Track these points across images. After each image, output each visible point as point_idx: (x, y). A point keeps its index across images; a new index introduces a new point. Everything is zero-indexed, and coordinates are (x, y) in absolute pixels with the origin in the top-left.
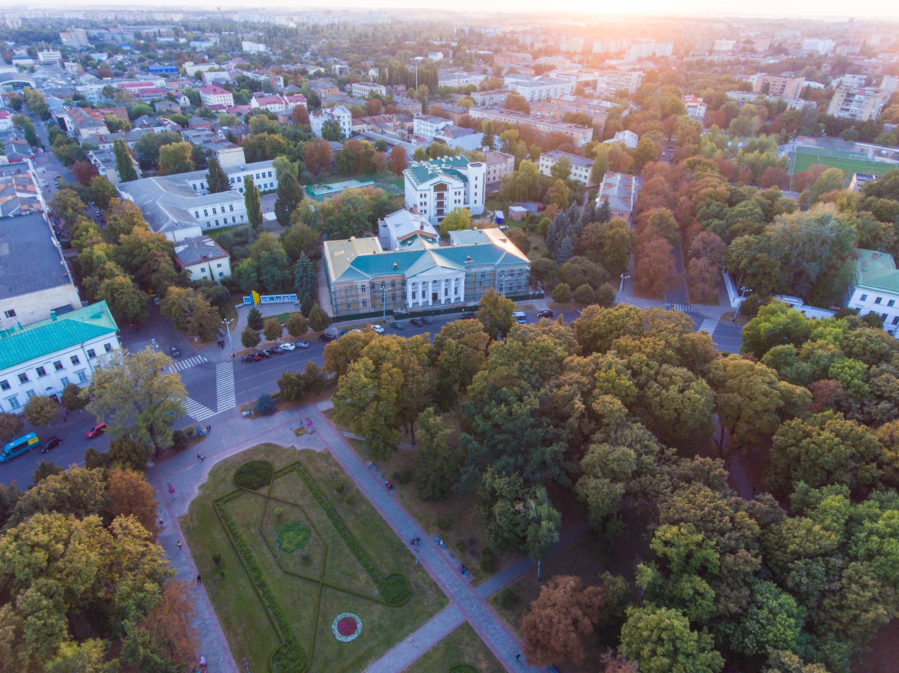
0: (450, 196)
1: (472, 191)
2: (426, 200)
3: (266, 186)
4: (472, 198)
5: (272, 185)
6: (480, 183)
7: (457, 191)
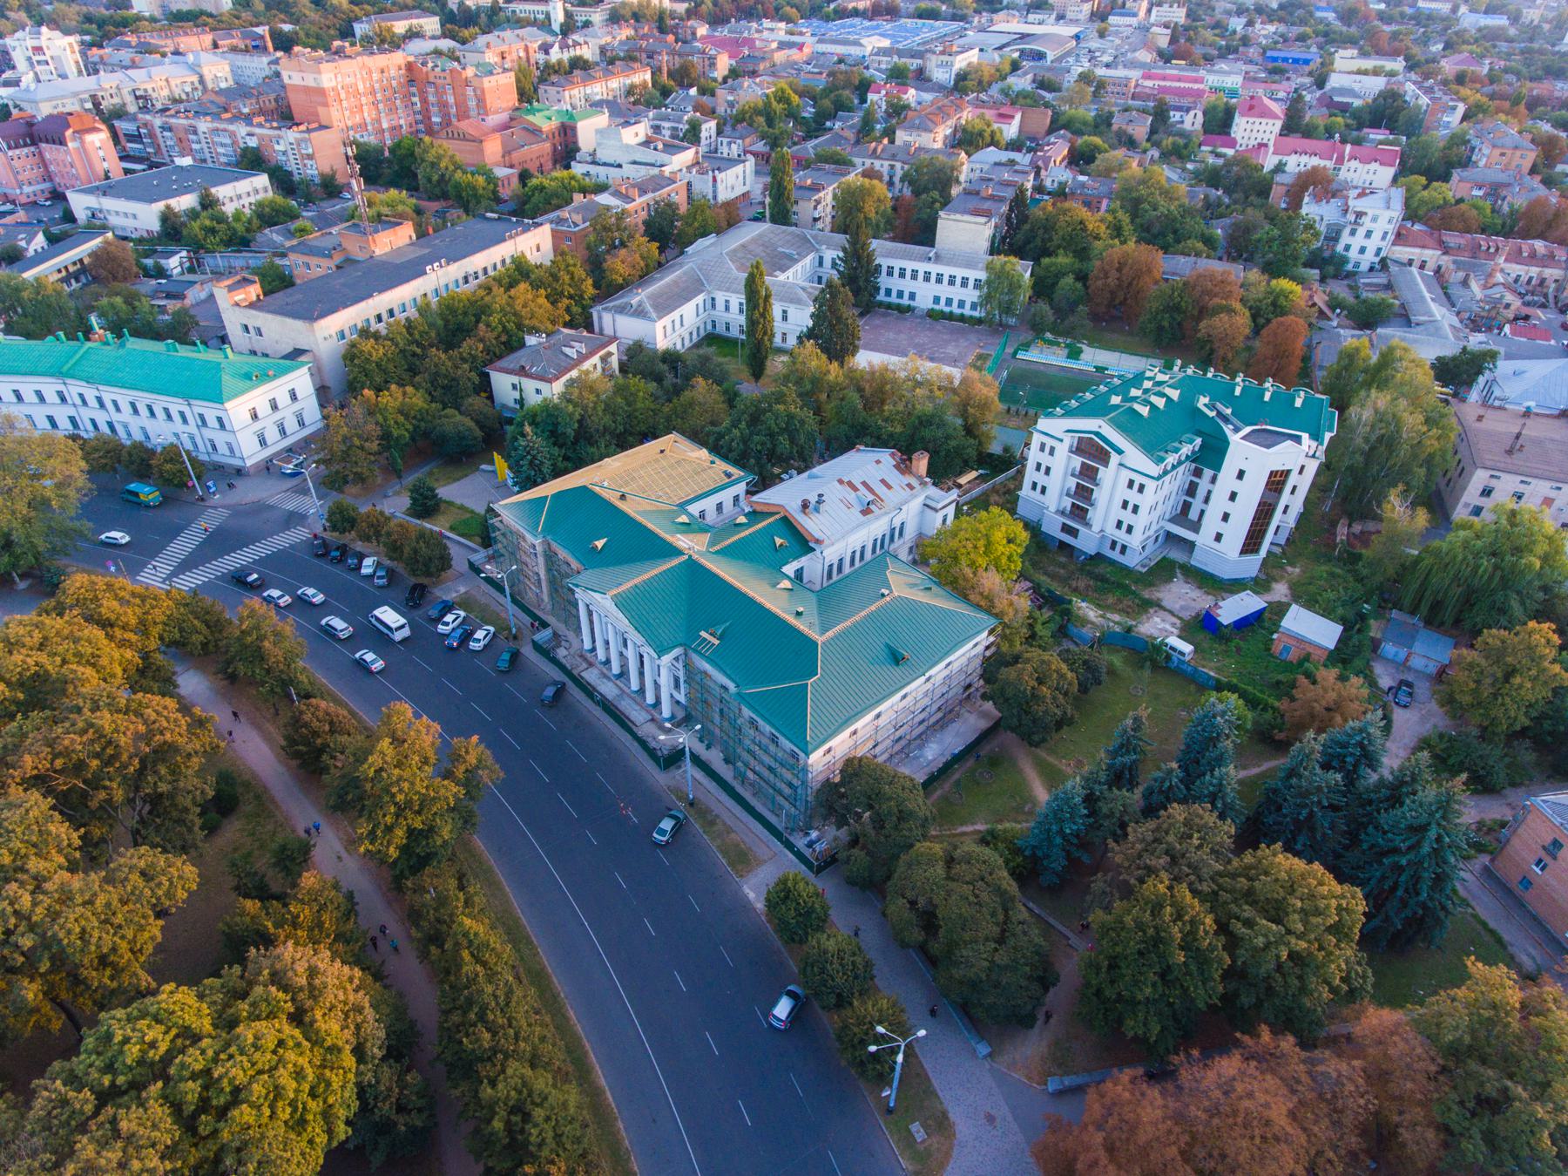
4: (1211, 524)
7: (1138, 479)
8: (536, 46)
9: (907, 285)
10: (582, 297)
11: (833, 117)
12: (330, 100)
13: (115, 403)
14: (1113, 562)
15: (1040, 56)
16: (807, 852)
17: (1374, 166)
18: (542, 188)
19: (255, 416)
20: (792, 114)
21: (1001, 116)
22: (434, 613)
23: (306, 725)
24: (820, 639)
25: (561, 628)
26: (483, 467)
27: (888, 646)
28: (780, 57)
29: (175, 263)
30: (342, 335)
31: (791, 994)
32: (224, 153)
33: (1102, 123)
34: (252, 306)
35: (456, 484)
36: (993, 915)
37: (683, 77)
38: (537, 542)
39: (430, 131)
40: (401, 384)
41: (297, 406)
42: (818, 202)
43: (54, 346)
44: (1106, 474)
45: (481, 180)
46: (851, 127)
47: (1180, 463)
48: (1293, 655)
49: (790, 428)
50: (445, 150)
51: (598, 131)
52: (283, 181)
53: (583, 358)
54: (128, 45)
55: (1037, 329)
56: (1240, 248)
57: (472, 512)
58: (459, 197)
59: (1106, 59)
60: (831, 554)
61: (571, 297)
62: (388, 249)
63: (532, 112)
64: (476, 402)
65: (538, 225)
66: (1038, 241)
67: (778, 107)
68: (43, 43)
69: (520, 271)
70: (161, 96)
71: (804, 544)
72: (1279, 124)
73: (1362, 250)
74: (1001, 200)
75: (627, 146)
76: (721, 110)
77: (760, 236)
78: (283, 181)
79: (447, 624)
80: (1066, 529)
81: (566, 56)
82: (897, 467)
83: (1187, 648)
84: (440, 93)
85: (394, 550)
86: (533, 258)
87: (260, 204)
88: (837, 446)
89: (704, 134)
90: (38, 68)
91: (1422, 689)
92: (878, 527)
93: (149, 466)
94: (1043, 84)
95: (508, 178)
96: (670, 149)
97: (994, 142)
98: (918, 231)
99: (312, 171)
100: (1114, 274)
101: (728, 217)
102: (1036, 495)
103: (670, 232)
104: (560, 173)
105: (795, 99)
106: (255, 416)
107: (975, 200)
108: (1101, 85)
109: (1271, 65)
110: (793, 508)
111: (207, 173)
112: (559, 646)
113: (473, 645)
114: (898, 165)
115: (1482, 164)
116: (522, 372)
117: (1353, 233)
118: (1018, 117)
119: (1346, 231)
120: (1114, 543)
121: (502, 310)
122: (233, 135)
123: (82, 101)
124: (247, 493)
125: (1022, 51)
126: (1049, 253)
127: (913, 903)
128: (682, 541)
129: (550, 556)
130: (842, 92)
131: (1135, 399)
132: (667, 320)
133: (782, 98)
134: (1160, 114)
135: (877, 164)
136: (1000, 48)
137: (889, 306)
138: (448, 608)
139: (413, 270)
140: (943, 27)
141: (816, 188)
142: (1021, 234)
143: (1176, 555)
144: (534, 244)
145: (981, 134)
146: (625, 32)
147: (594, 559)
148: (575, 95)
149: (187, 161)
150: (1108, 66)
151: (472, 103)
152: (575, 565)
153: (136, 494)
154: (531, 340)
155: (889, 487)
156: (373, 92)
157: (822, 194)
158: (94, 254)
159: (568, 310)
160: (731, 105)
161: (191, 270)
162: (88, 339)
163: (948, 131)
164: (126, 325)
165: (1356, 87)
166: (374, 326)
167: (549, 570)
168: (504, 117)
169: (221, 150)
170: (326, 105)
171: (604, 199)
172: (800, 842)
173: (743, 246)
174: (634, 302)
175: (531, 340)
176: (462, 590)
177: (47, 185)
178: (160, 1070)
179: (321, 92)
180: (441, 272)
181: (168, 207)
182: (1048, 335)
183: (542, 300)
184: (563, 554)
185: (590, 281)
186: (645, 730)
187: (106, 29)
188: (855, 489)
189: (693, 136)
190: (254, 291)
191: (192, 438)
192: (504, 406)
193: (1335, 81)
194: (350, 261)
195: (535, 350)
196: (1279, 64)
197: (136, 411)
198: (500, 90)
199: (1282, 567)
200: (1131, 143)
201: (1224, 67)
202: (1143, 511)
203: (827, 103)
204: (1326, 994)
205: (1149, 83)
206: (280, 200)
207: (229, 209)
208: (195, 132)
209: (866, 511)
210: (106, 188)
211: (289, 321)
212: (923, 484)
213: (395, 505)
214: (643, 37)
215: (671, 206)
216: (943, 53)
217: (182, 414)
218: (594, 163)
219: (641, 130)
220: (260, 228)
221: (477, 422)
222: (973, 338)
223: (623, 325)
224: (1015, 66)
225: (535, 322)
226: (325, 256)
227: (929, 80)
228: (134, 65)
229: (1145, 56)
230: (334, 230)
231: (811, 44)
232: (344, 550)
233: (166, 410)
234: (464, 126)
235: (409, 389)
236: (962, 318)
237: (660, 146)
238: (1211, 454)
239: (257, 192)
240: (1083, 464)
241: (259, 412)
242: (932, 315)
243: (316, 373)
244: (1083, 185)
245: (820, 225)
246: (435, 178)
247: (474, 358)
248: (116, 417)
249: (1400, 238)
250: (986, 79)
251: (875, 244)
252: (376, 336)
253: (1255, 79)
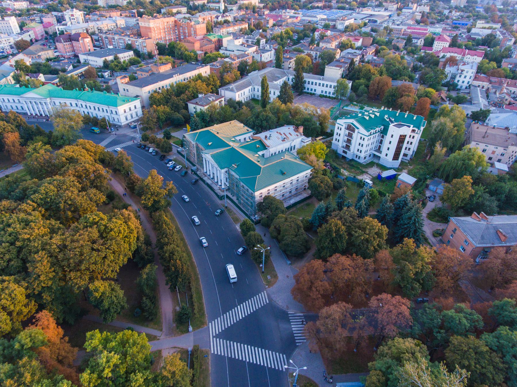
3: (326, 92)
4: (384, 149)
7: (363, 137)
8: (214, 16)
9: (314, 87)
10: (216, 85)
11: (303, 39)
12: (152, 31)
13: (90, 107)
14: (356, 161)
15: (376, 21)
17: (475, 57)
18: (209, 57)
19: (125, 112)
20: (290, 38)
21: (356, 39)
22: (166, 162)
23: (132, 180)
24: (262, 167)
25: (199, 167)
28: (290, 21)
29: (106, 74)
30: (149, 92)
32: (122, 45)
33: (388, 43)
34: (126, 83)
36: (295, 229)
37: (258, 26)
38: (194, 143)
39: (180, 40)
40: (164, 105)
41: (136, 110)
42: (290, 62)
43: (75, 92)
44: (355, 135)
45: (192, 54)
46: (308, 42)
47: (376, 133)
49: (267, 119)
50: (184, 45)
51: (228, 41)
52: (137, 53)
53: (214, 101)
54: (97, 15)
55: (351, 100)
56: (423, 81)
58: (186, 59)
59: (398, 23)
60: (272, 150)
61: (213, 85)
62: (164, 71)
63: (209, 35)
64: (184, 111)
65: (206, 66)
66: (356, 76)
67: (285, 35)
68: (74, 13)
69: (199, 77)
70: (105, 29)
71: (264, 147)
72: (448, 44)
73: (463, 82)
74: (346, 63)
75: (236, 45)
76: (268, 36)
77: (270, 71)
78: (137, 53)
81: (223, 19)
82: (294, 130)
84: (184, 29)
85: (158, 146)
86: (204, 75)
87: (130, 59)
88: (279, 124)
89: (261, 43)
90: (72, 21)
91: (438, 198)
92: (286, 145)
93: (98, 123)
94: (373, 30)
95: (201, 54)
96: (249, 46)
97: (352, 48)
98: (319, 71)
99: (145, 51)
100: (376, 85)
101: (263, 66)
102: (337, 142)
103: (244, 70)
104: (215, 53)
105: (291, 33)
106: (125, 112)
107: (339, 64)
108: (391, 30)
109: (454, 25)
111: (117, 50)
113: (176, 169)
114: (318, 53)
115: (514, 57)
116: (196, 103)
117: (460, 76)
118: (361, 40)
119: (458, 76)
120: (357, 156)
122: (124, 40)
123: (83, 30)
124: (121, 132)
125: (369, 20)
126: (358, 79)
128: (231, 144)
129: (197, 147)
130: (306, 33)
132: (239, 93)
133: (287, 33)
134: (409, 40)
135: (312, 52)
136: (362, 19)
137: (308, 93)
138: (171, 161)
139: (170, 76)
140: (345, 12)
141: (290, 58)
142: (352, 73)
143: (376, 161)
144: (205, 71)
145: (347, 45)
146: (242, 13)
147: (208, 147)
148: (224, 31)
149: (111, 47)
150: (398, 25)
151: (193, 33)
153: (94, 130)
154: (200, 96)
155: (291, 135)
156: (164, 29)
157: (292, 60)
158: (85, 71)
159: (212, 89)
160: (271, 35)
161: (111, 76)
162: (84, 90)
163: (337, 44)
164: (94, 87)
165: (481, 33)
166: (158, 90)
167: (197, 151)
168: (202, 37)
169: (121, 44)
170: (151, 32)
171: (227, 60)
175: (200, 96)
177: (73, 53)
178: (96, 223)
179: (150, 28)
180: (177, 77)
181: (106, 59)
182: (355, 103)
185: (219, 81)
187: (91, 9)
188: (281, 135)
189: (258, 43)
190: (127, 80)
191: (109, 117)
193: (474, 31)
194: (153, 74)
195: (201, 98)
196: (457, 25)
197: (95, 109)
198: (201, 29)
199: (407, 166)
200: (397, 49)
201: (437, 26)
202: (364, 146)
203: (301, 35)
204: (372, 248)
205: (409, 31)
206: (136, 58)
207: (122, 60)
208: (114, 39)
209: (283, 140)
210: (89, 54)
211: (136, 88)
212: (301, 135)
213: (160, 136)
214: (248, 14)
215: (246, 62)
216: (342, 20)
217: (106, 110)
218: (226, 50)
219: (240, 41)
220: (130, 66)
222: (331, 103)
223: (226, 94)
224: (365, 25)
225: (202, 91)
226: (146, 72)
227: (336, 28)
228: (98, 20)
229: (411, 22)
230: (150, 66)
231: (300, 16)
232: (145, 146)
233: (103, 109)
234: (189, 39)
235: (166, 106)
236: (329, 97)
237: (246, 46)
239: (130, 56)
240: (349, 133)
241: (126, 110)
242: (321, 96)
243: (142, 102)
244: (375, 60)
245: (291, 69)
246: (180, 53)
247: (184, 99)
248: (90, 111)
249: (476, 78)
250: (354, 28)
251: (304, 74)
252: (158, 93)
253: (447, 30)
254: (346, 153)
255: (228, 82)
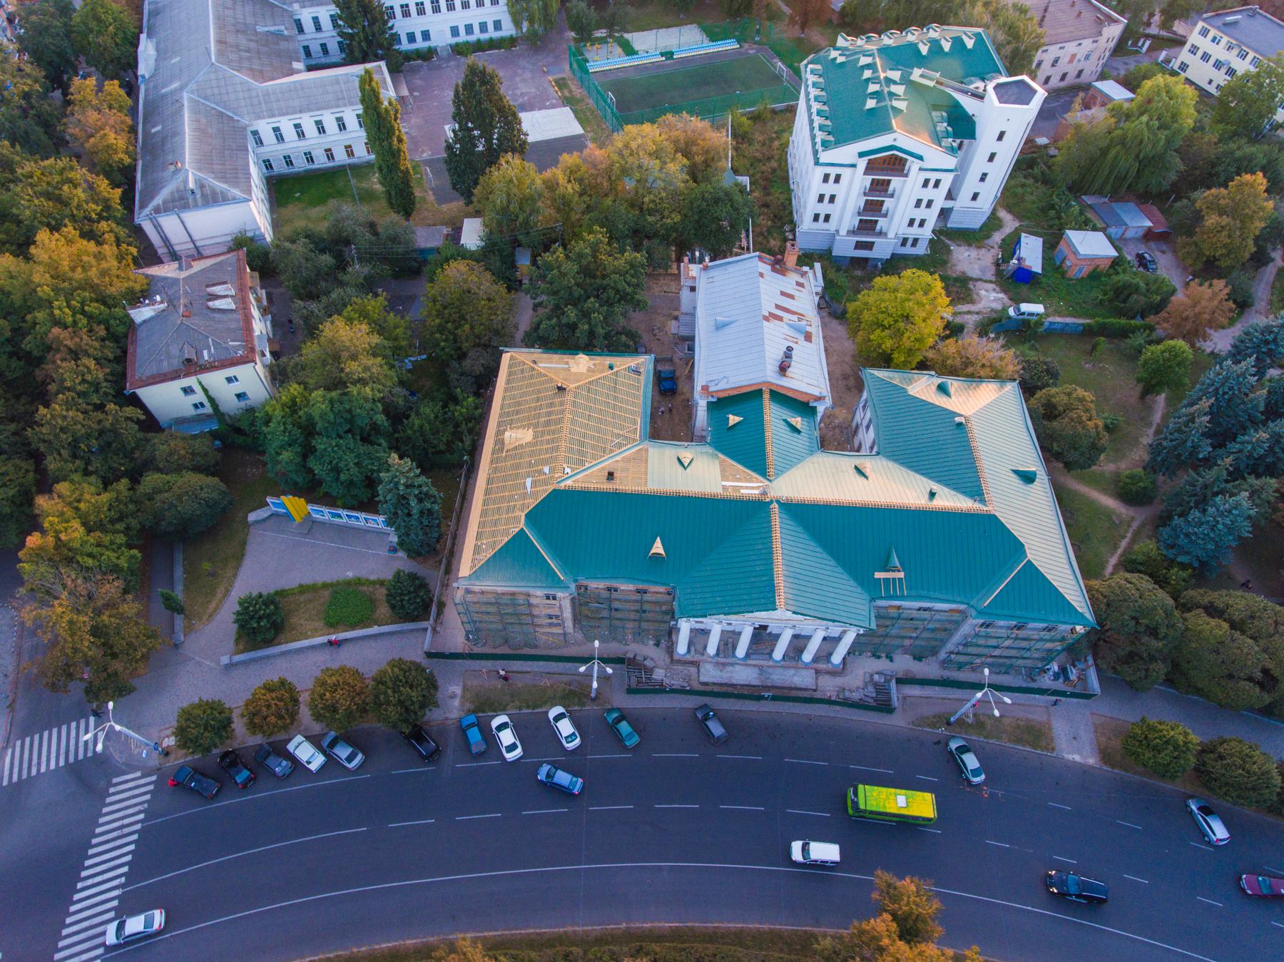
0: (906, 189)
1: (978, 164)
2: (839, 190)
3: (483, 27)
4: (970, 184)
5: (498, 25)
6: (1008, 152)
7: (933, 176)
9: (415, 24)
10: (107, 207)
16: (1059, 685)
26: (252, 517)
27: (1016, 472)
31: (1206, 811)
35: (249, 564)
48: (1086, 270)
57: (325, 586)
61: (101, 218)
71: (803, 406)
79: (512, 748)
80: (859, 245)
83: (1038, 308)
102: (821, 224)
110: (769, 375)
112: (649, 671)
116: (191, 367)
121: (56, 290)
127: (1250, 679)
131: (876, 95)
152: (626, 586)
154: (142, 314)
155: (792, 297)
172: (1046, 681)
173: (220, 42)
174: (191, 185)
176: (457, 689)
183: (91, 247)
184: (596, 585)
186: (829, 686)
192: (181, 421)
212: (804, 274)
221: (197, 469)
222: (522, 62)
232: (232, 760)
235: (63, 487)
238: (962, 127)
254: (869, 246)
255: (127, 161)
